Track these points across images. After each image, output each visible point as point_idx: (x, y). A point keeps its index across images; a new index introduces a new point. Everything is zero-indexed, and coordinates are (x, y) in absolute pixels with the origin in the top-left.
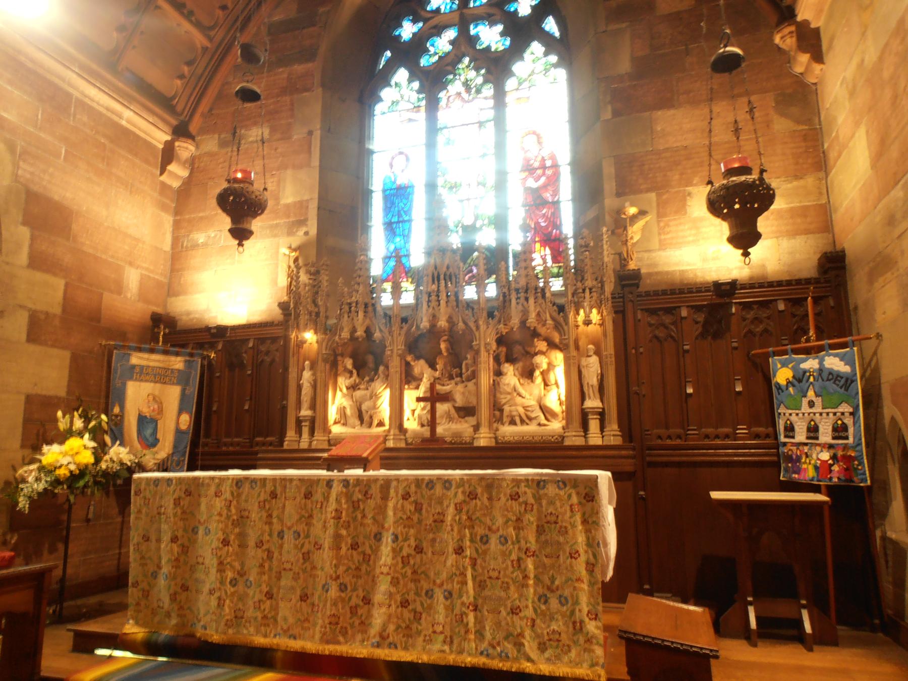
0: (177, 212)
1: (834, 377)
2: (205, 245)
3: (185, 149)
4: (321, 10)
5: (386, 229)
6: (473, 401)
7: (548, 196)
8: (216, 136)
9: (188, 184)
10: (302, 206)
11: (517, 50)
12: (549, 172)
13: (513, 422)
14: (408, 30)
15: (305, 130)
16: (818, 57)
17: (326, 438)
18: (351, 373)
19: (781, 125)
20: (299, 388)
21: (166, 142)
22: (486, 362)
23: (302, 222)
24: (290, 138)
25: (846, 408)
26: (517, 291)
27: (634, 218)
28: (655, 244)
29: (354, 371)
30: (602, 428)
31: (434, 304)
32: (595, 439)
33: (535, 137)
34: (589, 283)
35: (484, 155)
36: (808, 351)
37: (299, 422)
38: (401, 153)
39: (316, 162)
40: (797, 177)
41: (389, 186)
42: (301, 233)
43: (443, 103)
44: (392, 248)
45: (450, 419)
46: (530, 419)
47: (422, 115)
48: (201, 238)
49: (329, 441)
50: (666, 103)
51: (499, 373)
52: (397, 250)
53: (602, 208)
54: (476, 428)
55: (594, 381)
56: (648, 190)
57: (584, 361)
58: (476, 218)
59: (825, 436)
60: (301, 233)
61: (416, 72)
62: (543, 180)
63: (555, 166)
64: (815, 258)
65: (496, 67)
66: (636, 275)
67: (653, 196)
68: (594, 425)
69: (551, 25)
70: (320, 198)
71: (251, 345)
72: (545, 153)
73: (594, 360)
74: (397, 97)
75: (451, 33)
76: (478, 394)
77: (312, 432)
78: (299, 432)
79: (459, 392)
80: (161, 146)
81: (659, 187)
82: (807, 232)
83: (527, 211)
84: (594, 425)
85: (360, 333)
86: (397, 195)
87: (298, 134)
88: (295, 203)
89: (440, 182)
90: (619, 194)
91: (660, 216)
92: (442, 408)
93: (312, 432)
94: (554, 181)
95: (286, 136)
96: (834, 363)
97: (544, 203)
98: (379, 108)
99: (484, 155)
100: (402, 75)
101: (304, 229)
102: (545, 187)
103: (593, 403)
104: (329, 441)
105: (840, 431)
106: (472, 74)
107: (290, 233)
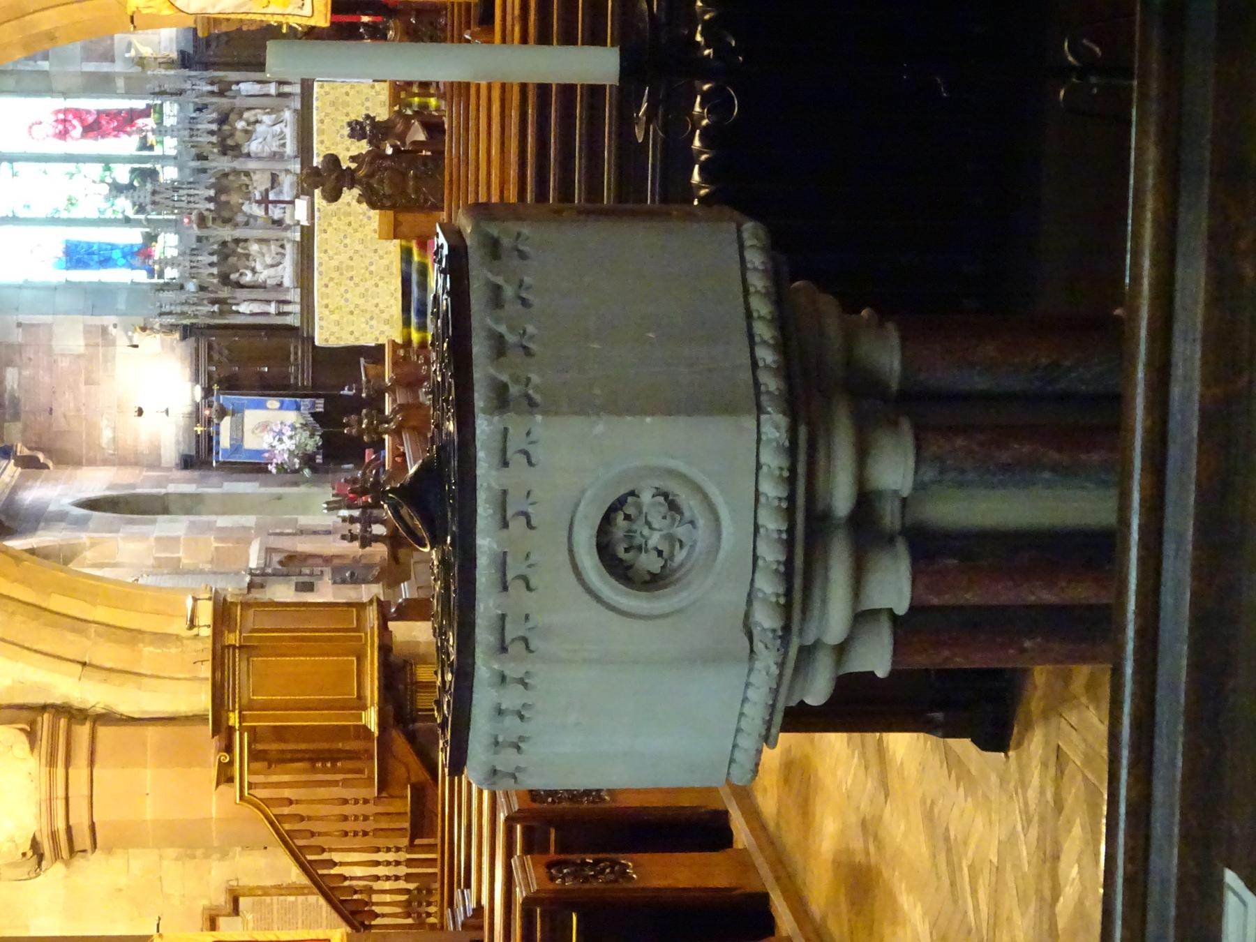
0: (77, 462)
2: (114, 429)
3: (22, 450)
5: (105, 267)
6: (268, 176)
7: (90, 119)
8: (6, 425)
9: (49, 452)
10: (88, 331)
12: (70, 117)
13: (284, 145)
15: (16, 330)
18: (241, 275)
20: (253, 314)
21: (16, 465)
22: (238, 164)
23: (104, 330)
24: (20, 345)
26: (191, 136)
27: (137, 50)
31: (196, 199)
33: (35, 127)
34: (188, 86)
35: (45, 172)
37: (280, 314)
39: (47, 319)
44: (122, 261)
45: (281, 192)
46: (282, 132)
48: (106, 435)
51: (248, 155)
52: (124, 256)
53: (119, 74)
54: (288, 171)
55: (258, 86)
56: (112, 38)
57: (244, 93)
58: (102, 181)
62: (75, 122)
63: (66, 111)
66: (182, 53)
67: (117, 37)
68: (286, 89)
70: (84, 314)
71: (214, 369)
73: (243, 86)
76: (263, 170)
77: (288, 302)
79: (260, 183)
80: (19, 469)
83: (103, 137)
84: (286, 89)
85: (215, 259)
87: (18, 337)
88: (86, 338)
89: (64, 215)
90: (113, 61)
92: (272, 197)
93: (288, 302)
94: (78, 114)
95: (19, 348)
99: (45, 172)
101: (111, 328)
102: (82, 121)
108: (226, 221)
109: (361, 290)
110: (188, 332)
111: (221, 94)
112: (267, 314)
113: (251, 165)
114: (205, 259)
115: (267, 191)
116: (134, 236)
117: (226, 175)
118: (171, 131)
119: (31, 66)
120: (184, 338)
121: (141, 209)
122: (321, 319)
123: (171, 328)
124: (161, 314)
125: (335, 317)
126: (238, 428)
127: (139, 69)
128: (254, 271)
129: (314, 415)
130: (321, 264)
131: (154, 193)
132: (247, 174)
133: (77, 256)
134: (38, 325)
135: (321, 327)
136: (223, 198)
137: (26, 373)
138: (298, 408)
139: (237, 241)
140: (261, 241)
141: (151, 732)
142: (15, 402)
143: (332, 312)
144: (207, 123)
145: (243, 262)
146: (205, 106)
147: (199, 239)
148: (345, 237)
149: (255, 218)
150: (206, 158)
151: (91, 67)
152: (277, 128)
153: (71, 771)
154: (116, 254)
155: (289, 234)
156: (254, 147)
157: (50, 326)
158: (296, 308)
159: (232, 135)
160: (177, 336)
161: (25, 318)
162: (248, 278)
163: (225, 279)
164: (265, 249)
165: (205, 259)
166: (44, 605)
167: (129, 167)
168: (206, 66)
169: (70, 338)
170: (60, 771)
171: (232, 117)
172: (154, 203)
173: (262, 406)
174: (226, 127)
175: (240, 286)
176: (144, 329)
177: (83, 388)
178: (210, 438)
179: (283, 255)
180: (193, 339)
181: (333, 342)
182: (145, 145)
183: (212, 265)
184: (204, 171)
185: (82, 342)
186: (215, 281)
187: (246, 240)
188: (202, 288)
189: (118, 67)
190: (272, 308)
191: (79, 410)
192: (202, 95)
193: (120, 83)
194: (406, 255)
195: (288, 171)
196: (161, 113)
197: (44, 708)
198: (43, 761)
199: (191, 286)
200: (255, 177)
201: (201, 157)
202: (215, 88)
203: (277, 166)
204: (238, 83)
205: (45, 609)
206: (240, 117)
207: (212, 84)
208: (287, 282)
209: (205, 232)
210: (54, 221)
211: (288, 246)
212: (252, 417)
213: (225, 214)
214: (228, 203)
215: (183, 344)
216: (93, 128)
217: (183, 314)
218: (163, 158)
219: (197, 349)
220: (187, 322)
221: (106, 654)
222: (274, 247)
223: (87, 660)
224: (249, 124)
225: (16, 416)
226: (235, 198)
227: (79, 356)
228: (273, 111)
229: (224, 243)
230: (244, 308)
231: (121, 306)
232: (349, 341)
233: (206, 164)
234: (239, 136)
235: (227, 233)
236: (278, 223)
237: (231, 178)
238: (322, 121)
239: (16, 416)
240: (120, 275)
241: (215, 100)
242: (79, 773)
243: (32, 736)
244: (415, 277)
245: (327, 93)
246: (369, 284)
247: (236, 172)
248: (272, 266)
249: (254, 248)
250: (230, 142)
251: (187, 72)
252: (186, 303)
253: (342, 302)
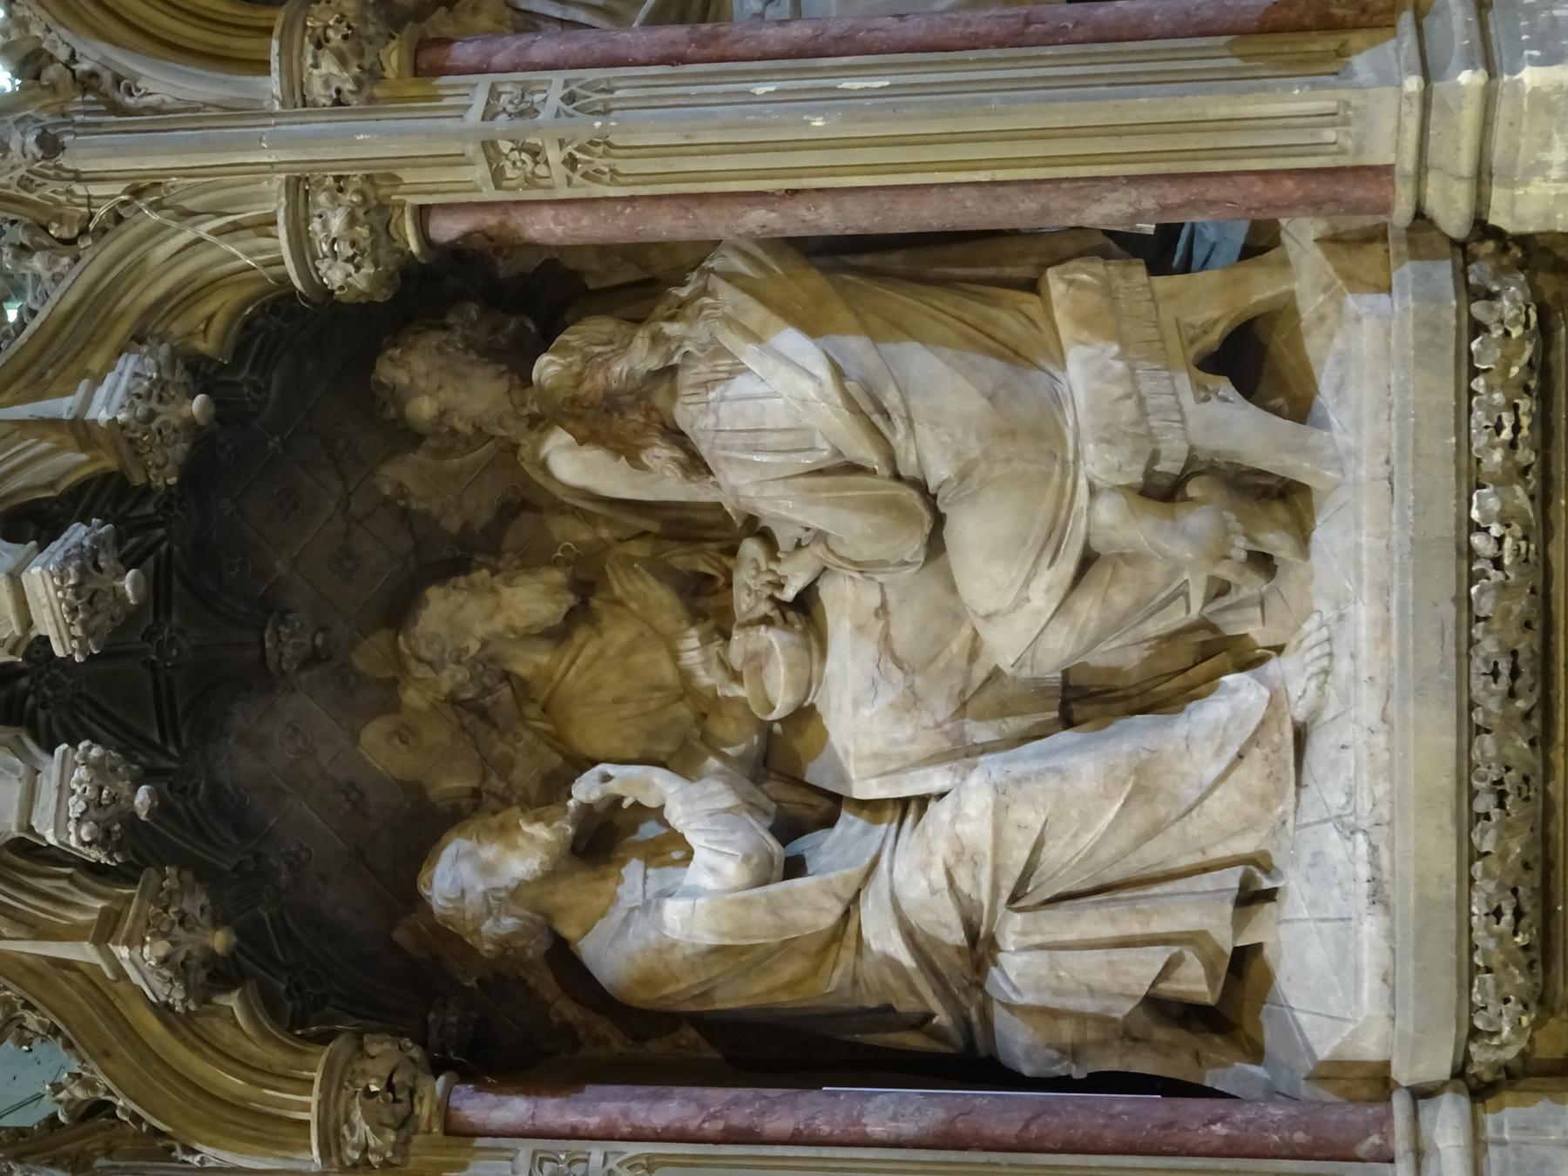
17: (1447, 1126)
18: (604, 839)
29: (586, 789)
49: (1479, 1088)
104: (1479, 1088)
128: (794, 799)
139: (507, 293)
140: (872, 267)
145: (646, 645)
164: (942, 396)
175: (541, 1021)
179: (1280, 498)
186: (140, 963)
187: (638, 282)
222: (1100, 372)
229: (294, 370)
249: (769, 396)
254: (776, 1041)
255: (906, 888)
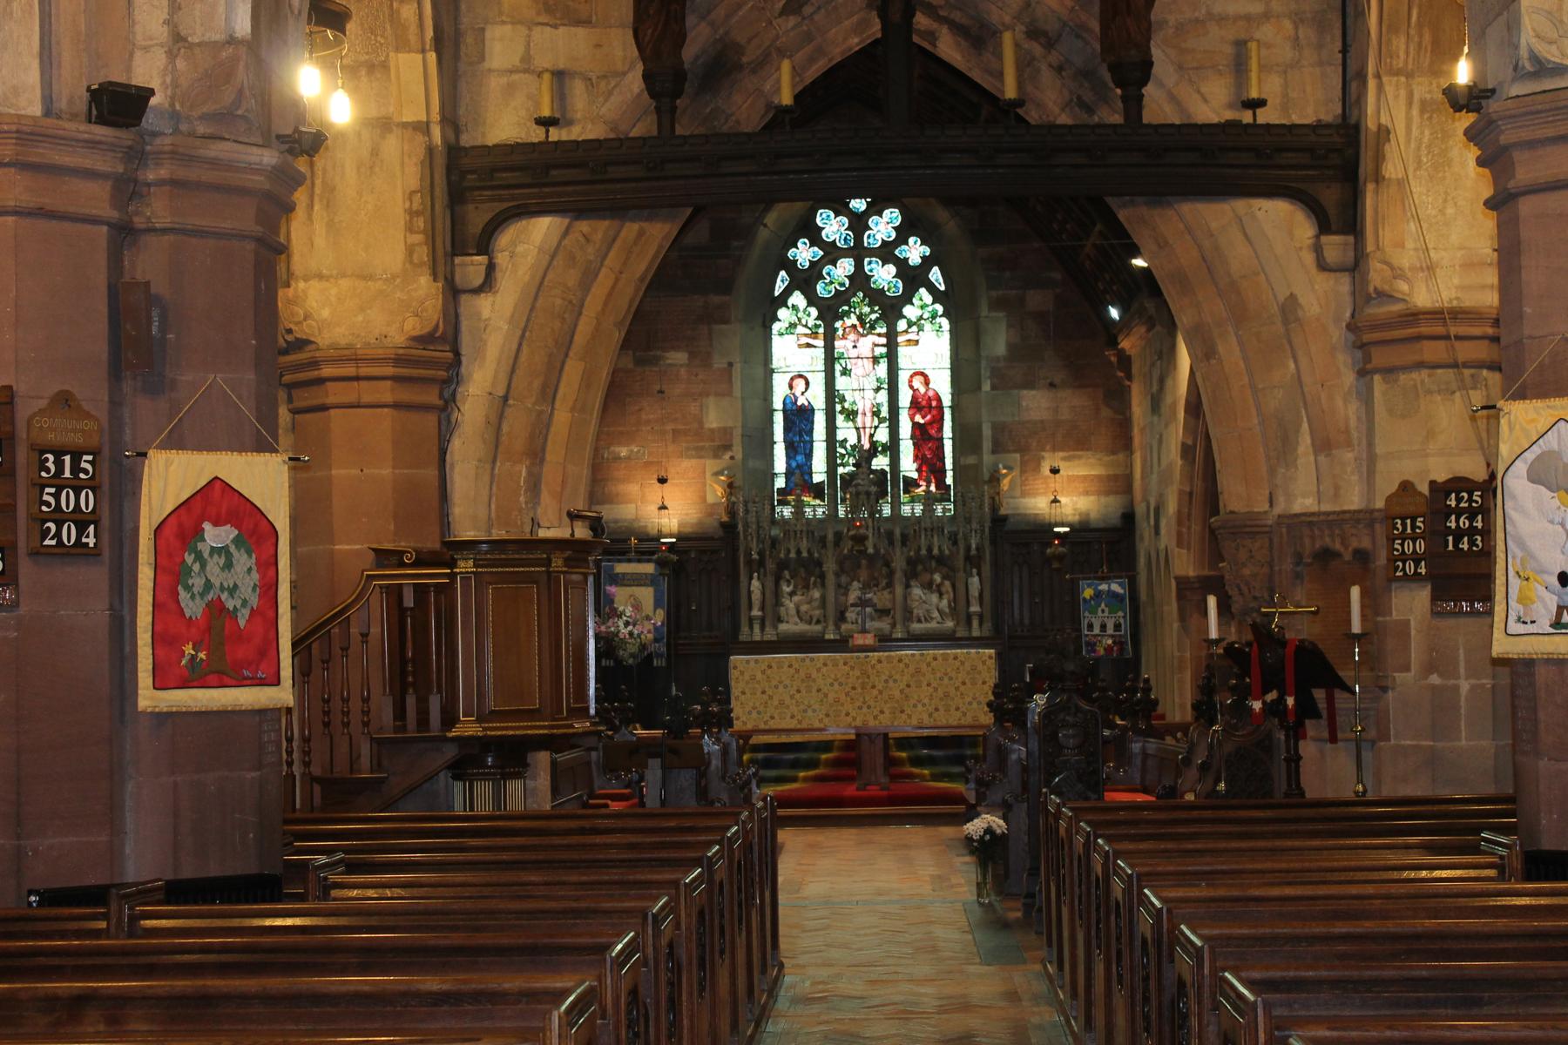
1: (1114, 595)
2: (628, 458)
4: (736, 244)
6: (889, 605)
7: (933, 432)
10: (726, 432)
11: (907, 298)
12: (934, 412)
13: (919, 621)
14: (804, 253)
16: (1129, 377)
19: (1106, 412)
20: (750, 593)
22: (898, 575)
23: (728, 447)
25: (1120, 614)
27: (1005, 475)
28: (1018, 493)
30: (981, 624)
32: (976, 633)
33: (921, 378)
34: (974, 526)
36: (1103, 579)
37: (751, 620)
38: (801, 376)
40: (1114, 453)
41: (789, 406)
42: (727, 457)
43: (840, 332)
44: (794, 464)
45: (872, 619)
47: (820, 343)
50: (1029, 385)
51: (908, 586)
54: (894, 625)
59: (1110, 631)
60: (727, 457)
61: (812, 300)
63: (940, 407)
64: (1119, 514)
65: (890, 308)
66: (1005, 519)
67: (1018, 456)
68: (975, 623)
69: (935, 275)
72: (931, 393)
73: (976, 579)
74: (794, 319)
75: (845, 267)
76: (894, 600)
78: (751, 627)
79: (880, 598)
81: (1022, 449)
82: (1117, 493)
84: (975, 623)
86: (799, 417)
87: (719, 363)
88: (719, 429)
89: (838, 408)
90: (994, 452)
91: (1023, 472)
94: (939, 420)
96: (1115, 587)
97: (931, 438)
98: (776, 327)
99: (878, 390)
100: (797, 299)
103: (975, 608)
105: (1117, 627)
106: (866, 309)
107: (716, 456)
108: (841, 563)
109: (788, 701)
110: (729, 528)
111: (968, 558)
112: (750, 608)
113: (899, 590)
114: (804, 545)
115: (874, 606)
116: (819, 474)
117: (887, 564)
118: (929, 509)
119: (985, 373)
120: (723, 525)
121: (848, 480)
122: (756, 661)
123: (731, 510)
124: (746, 503)
125: (759, 676)
126: (638, 580)
127: (986, 477)
128: (792, 594)
129: (650, 656)
130: (812, 660)
131: (868, 494)
132: (890, 585)
133: (799, 417)
134: (730, 381)
135: (748, 662)
136: (864, 562)
137: (683, 371)
138: (656, 640)
139: (822, 576)
141: (432, 473)
142: (655, 361)
143: (763, 672)
144: (939, 545)
146: (955, 543)
147: (823, 540)
148: (841, 684)
149: (846, 594)
150: (904, 543)
151: (987, 431)
152: (936, 614)
153: (389, 383)
154: (800, 458)
155: (831, 627)
156: (917, 592)
157: (729, 393)
158: (757, 638)
159: (925, 570)
160: (725, 519)
161: (737, 367)
162: (787, 589)
163: (783, 565)
164: (816, 604)
165: (804, 545)
166: (571, 354)
167: (887, 469)
168: (993, 542)
169: (715, 416)
170: (389, 371)
171: (945, 570)
172: (858, 494)
173: (657, 605)
174: (934, 564)
176: (730, 486)
177: (669, 427)
178: (624, 554)
180: (720, 533)
181: (734, 674)
182: (910, 484)
183: (799, 552)
184: (891, 543)
185: (714, 425)
187: (823, 585)
188: (774, 542)
189: (987, 458)
190: (756, 612)
191: (648, 422)
192: (966, 538)
193: (971, 460)
194: (826, 746)
195: (894, 625)
196: (941, 500)
197: (457, 354)
198: (401, 351)
199: (775, 532)
200: (885, 593)
201: (905, 539)
202: (973, 552)
203: (899, 615)
204: (979, 574)
205: (567, 355)
206: (944, 578)
207: (977, 549)
208: (783, 627)
209: (830, 545)
210: (832, 394)
211: (818, 628)
212: (646, 595)
213: (848, 567)
214: (859, 567)
215: (716, 524)
216: (926, 437)
217: (746, 525)
218: (896, 504)
219: (712, 539)
220: (740, 527)
221: (517, 424)
223: (511, 402)
224: (939, 586)
225: (639, 362)
226: (864, 574)
227: (701, 423)
228: (954, 610)
229: (819, 564)
230: (755, 584)
231: (751, 464)
232: (736, 690)
233: (898, 544)
234: (926, 577)
235: (830, 566)
236: (841, 617)
237: (884, 571)
238: (956, 658)
239: (639, 362)
240: (780, 464)
241: (962, 552)
242: (385, 392)
243: (424, 340)
244: (804, 756)
245: (984, 663)
246: (794, 709)
247: (891, 574)
248: (798, 612)
249: (817, 594)
250: (920, 568)
251: (987, 525)
252: (759, 527)
253: (774, 683)
254: (777, 594)
255: (786, 601)
